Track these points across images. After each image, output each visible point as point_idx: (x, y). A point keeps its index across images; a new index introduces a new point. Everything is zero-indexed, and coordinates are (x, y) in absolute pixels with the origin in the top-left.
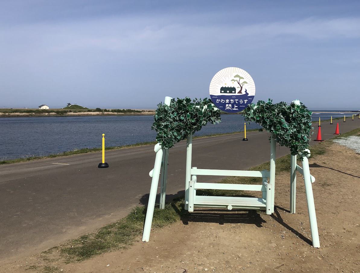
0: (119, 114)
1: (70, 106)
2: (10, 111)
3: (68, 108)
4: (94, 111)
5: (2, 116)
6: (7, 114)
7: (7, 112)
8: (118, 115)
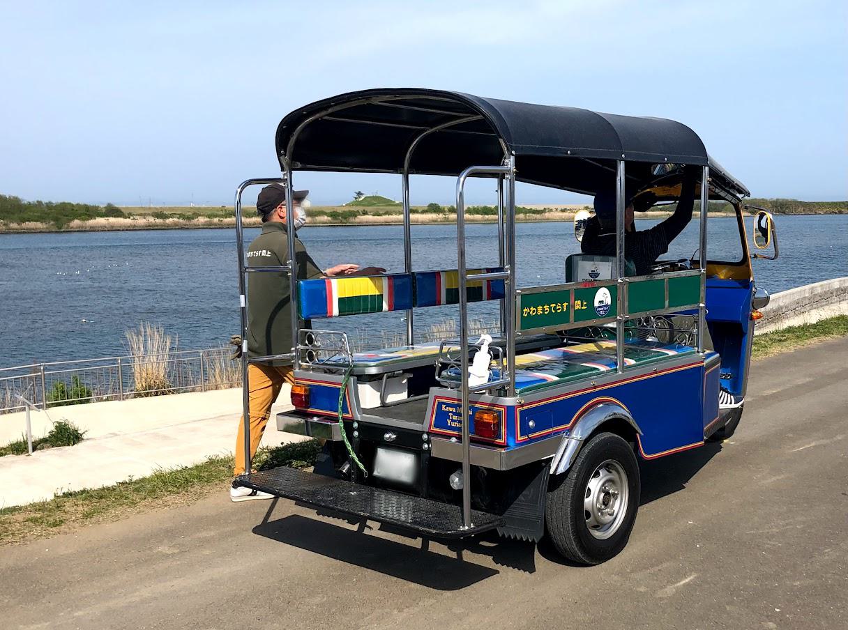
0: (488, 220)
1: (363, 198)
2: (221, 213)
3: (357, 203)
4: (424, 212)
5: (205, 225)
6: (216, 220)
7: (216, 216)
8: (485, 221)
